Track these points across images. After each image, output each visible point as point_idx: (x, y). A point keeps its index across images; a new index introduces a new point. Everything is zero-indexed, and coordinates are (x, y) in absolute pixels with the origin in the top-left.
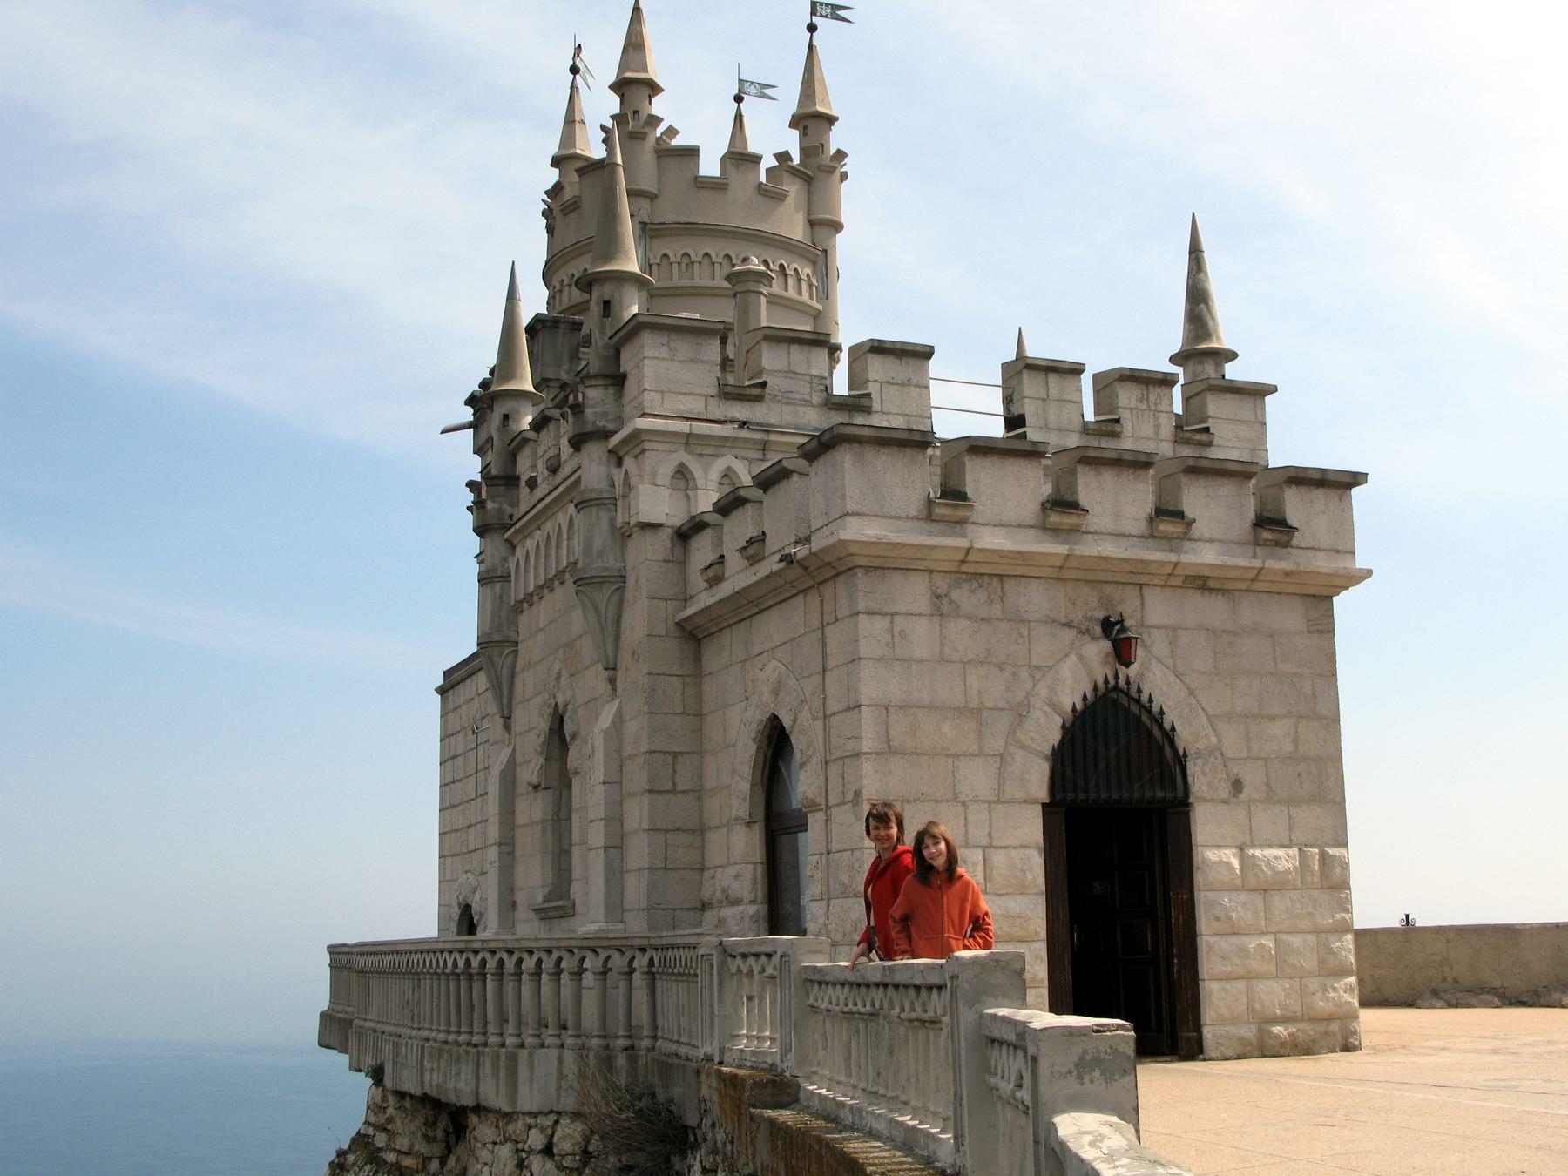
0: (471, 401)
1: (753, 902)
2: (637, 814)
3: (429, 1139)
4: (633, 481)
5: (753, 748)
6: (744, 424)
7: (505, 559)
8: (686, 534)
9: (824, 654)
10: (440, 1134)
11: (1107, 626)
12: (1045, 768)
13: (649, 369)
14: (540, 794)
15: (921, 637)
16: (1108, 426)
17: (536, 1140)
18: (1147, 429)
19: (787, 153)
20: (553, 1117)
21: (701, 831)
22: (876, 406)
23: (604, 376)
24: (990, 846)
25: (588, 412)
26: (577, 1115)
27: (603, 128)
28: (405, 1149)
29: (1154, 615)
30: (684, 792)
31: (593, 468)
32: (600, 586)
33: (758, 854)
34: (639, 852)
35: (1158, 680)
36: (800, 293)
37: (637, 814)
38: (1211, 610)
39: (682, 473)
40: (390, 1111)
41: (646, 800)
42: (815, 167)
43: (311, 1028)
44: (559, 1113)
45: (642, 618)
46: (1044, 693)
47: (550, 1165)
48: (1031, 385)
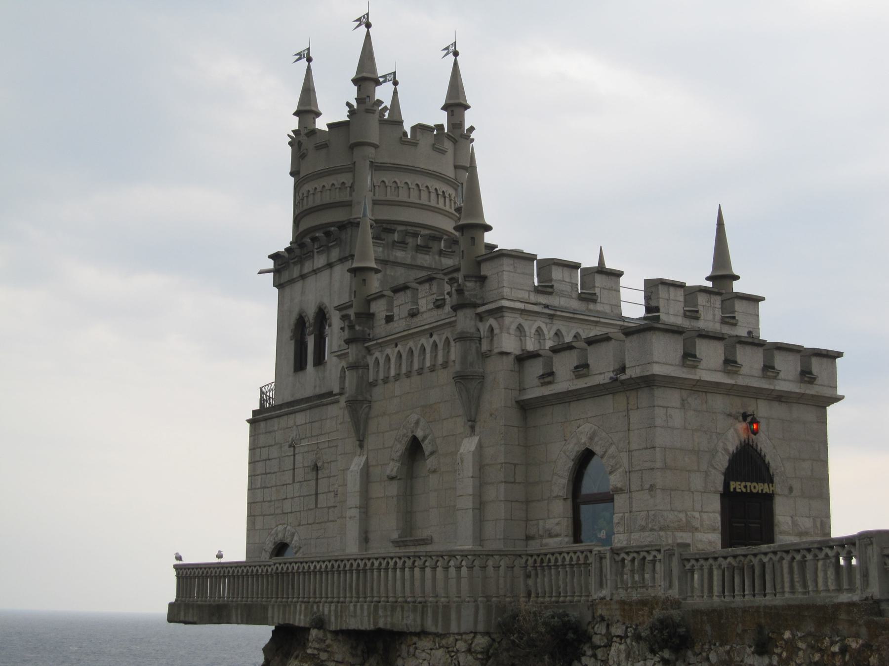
0: (275, 257)
1: (566, 536)
2: (495, 493)
3: (353, 656)
4: (496, 331)
5: (571, 464)
6: (547, 306)
7: (365, 357)
8: (523, 358)
9: (629, 424)
10: (359, 652)
11: (745, 416)
12: (723, 477)
13: (505, 276)
14: (395, 482)
15: (677, 418)
16: (693, 314)
17: (461, 646)
18: (710, 317)
19: (442, 125)
20: (472, 635)
21: (527, 502)
22: (599, 300)
23: (476, 277)
24: (702, 511)
25: (466, 293)
26: (487, 633)
27: (348, 104)
28: (340, 660)
29: (762, 410)
30: (519, 483)
31: (465, 321)
32: (469, 382)
33: (570, 513)
34: (497, 511)
35: (765, 443)
36: (445, 205)
37: (495, 493)
38: (779, 411)
39: (520, 328)
40: (328, 642)
41: (502, 486)
42: (454, 135)
43: (165, 611)
44: (475, 633)
45: (497, 398)
46: (721, 445)
47: (470, 657)
48: (662, 292)
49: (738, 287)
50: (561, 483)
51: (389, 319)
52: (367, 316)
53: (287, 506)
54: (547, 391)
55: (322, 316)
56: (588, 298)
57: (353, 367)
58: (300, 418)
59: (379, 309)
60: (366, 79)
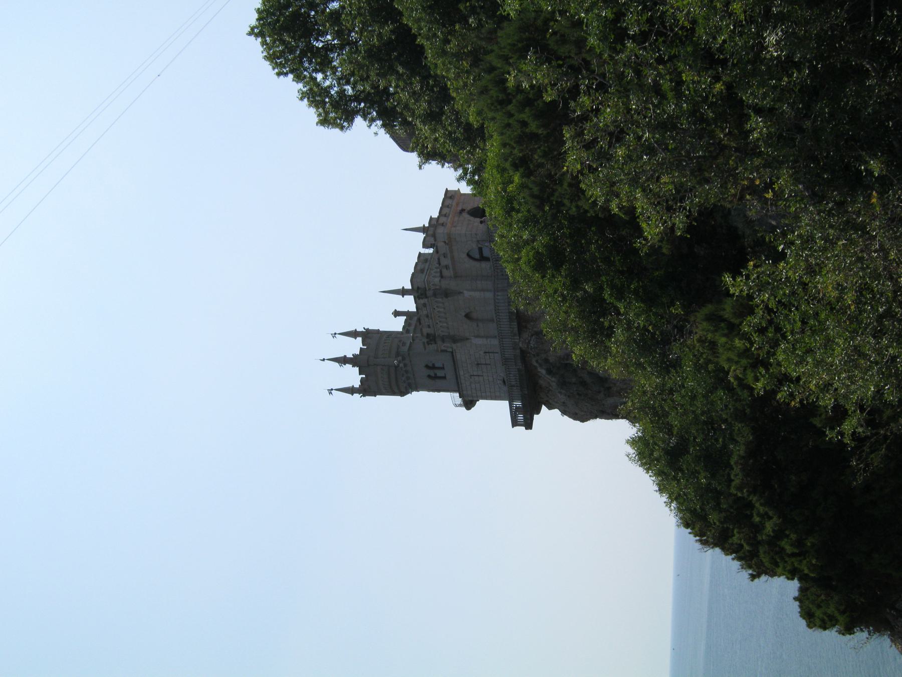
8: (442, 277)
29: (460, 208)
31: (430, 293)
32: (447, 294)
35: (469, 207)
49: (427, 225)
50: (477, 264)
51: (429, 326)
52: (428, 336)
53: (491, 379)
54: (451, 266)
55: (427, 366)
56: (426, 261)
57: (443, 341)
58: (461, 373)
59: (426, 331)
60: (343, 361)
